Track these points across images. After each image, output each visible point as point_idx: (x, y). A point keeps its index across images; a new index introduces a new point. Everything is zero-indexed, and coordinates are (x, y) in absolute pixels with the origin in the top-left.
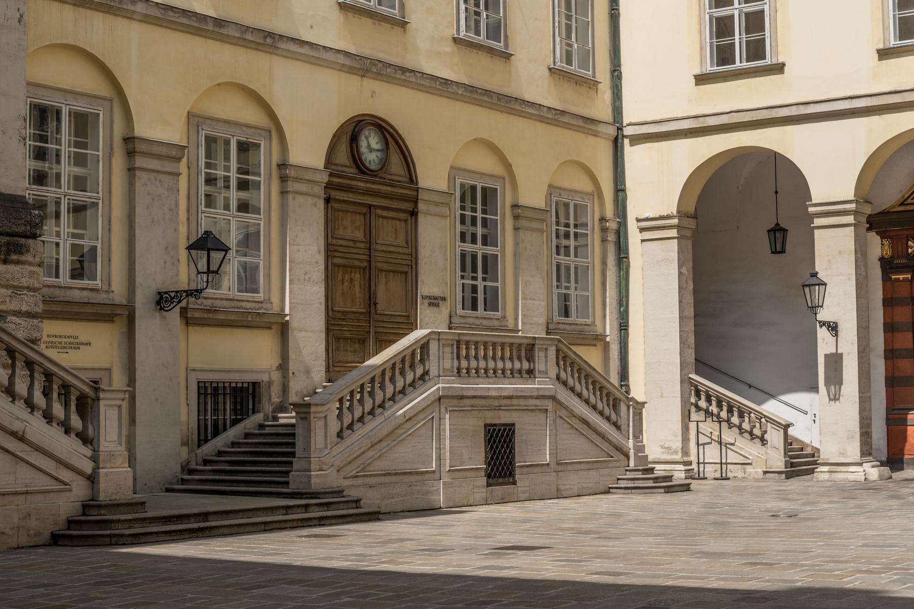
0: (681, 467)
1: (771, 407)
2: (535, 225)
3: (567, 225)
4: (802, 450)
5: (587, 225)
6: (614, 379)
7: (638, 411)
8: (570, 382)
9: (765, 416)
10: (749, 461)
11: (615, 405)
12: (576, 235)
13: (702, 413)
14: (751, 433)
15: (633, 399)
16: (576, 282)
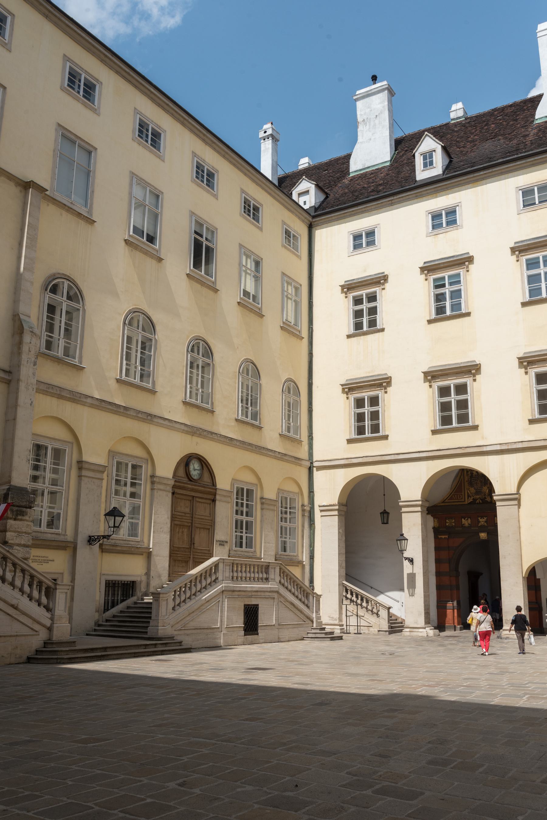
0: (338, 627)
1: (382, 599)
2: (272, 507)
3: (286, 508)
4: (396, 620)
5: (295, 508)
6: (307, 583)
7: (318, 599)
8: (286, 584)
9: (379, 603)
10: (371, 625)
11: (307, 597)
12: (290, 512)
13: (349, 601)
14: (372, 611)
15: (316, 593)
16: (290, 535)
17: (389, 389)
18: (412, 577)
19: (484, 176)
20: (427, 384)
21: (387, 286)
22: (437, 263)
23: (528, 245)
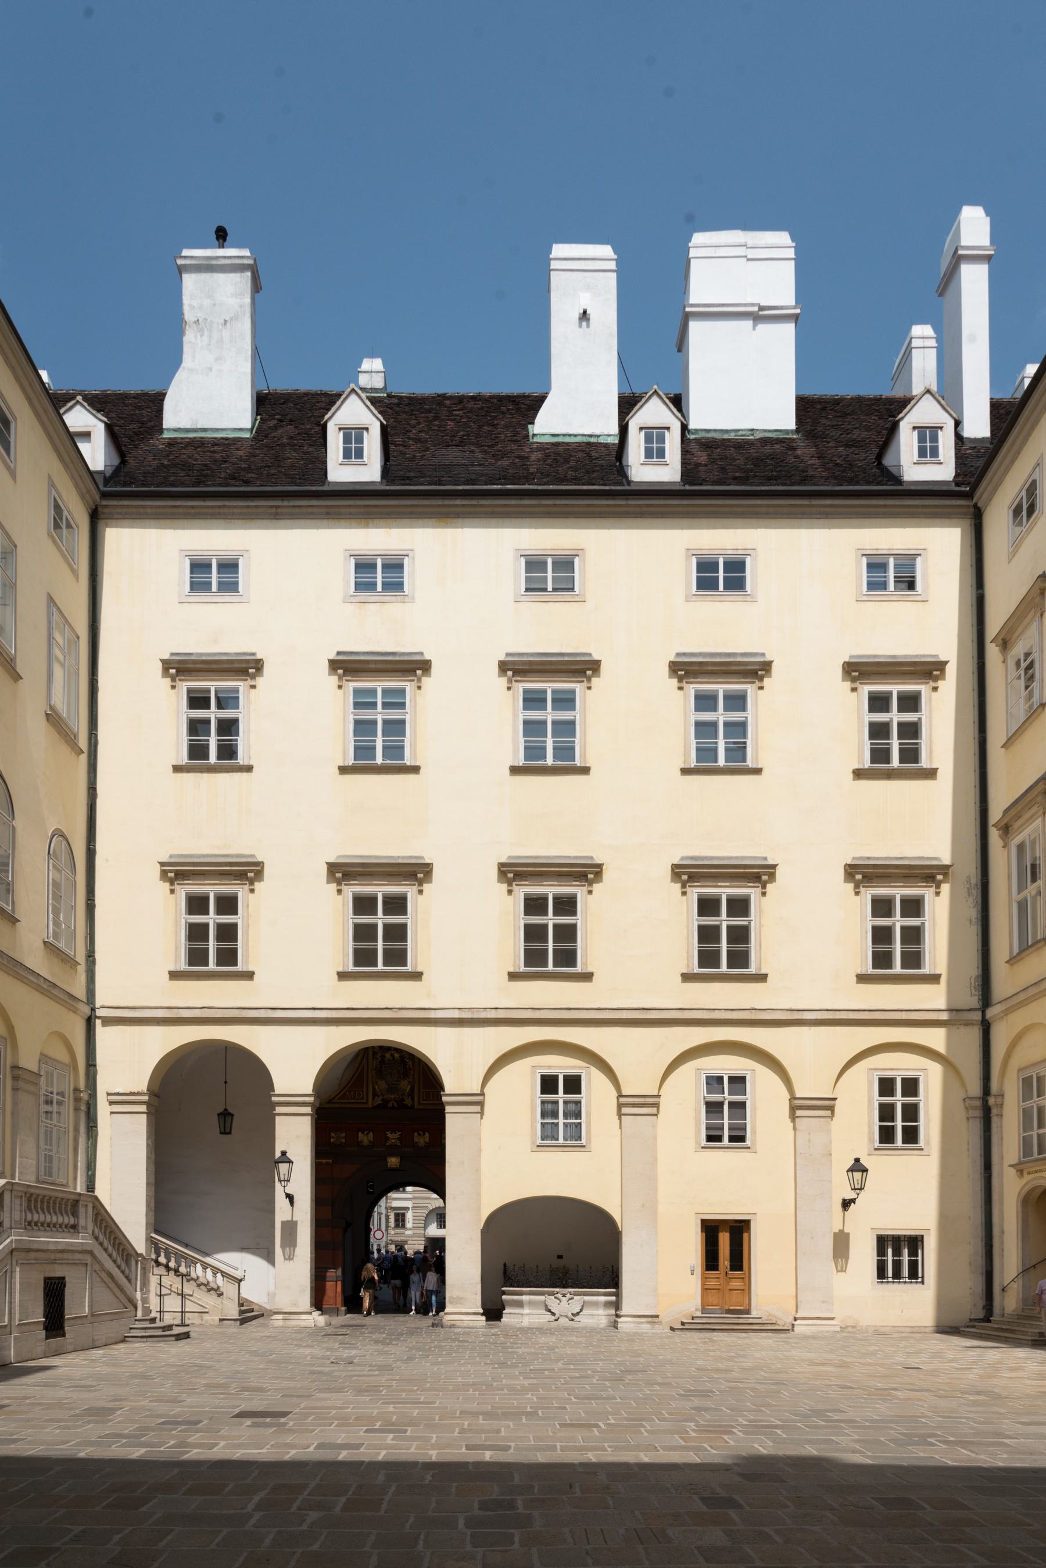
10: (207, 1310)
17: (257, 886)
18: (290, 1228)
19: (460, 509)
20: (334, 887)
21: (259, 681)
22: (362, 658)
23: (531, 663)
